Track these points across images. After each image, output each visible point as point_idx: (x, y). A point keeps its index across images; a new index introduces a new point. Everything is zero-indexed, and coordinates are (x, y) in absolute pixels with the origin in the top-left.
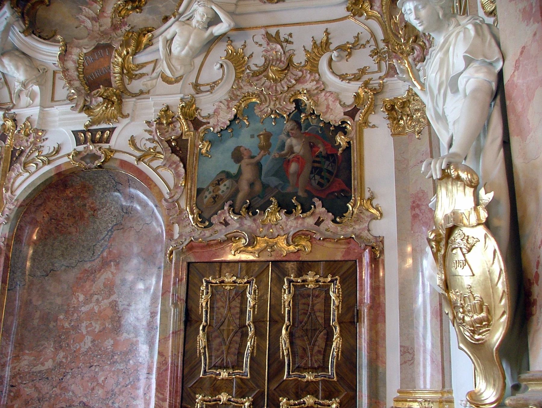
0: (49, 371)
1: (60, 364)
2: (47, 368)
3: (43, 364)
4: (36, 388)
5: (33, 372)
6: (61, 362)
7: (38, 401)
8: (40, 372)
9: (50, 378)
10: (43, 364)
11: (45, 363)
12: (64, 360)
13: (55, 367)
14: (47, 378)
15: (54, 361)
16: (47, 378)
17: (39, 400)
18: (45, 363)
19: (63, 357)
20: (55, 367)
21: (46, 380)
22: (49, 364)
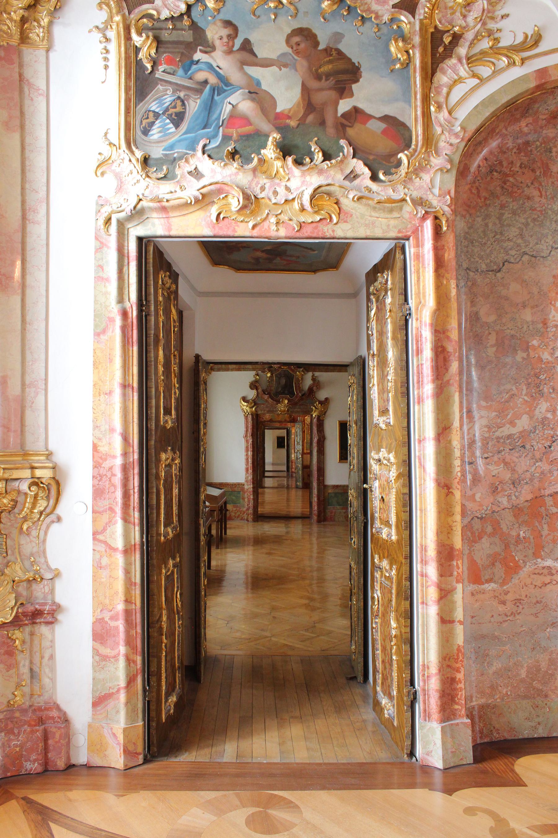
0: (524, 435)
1: (544, 422)
2: (521, 429)
3: (512, 423)
4: (506, 464)
5: (498, 438)
6: (546, 418)
8: (509, 437)
9: (528, 447)
10: (512, 423)
12: (549, 415)
13: (535, 428)
14: (524, 447)
15: (531, 418)
16: (524, 447)
19: (547, 411)
20: (535, 428)
21: (522, 449)
22: (524, 423)
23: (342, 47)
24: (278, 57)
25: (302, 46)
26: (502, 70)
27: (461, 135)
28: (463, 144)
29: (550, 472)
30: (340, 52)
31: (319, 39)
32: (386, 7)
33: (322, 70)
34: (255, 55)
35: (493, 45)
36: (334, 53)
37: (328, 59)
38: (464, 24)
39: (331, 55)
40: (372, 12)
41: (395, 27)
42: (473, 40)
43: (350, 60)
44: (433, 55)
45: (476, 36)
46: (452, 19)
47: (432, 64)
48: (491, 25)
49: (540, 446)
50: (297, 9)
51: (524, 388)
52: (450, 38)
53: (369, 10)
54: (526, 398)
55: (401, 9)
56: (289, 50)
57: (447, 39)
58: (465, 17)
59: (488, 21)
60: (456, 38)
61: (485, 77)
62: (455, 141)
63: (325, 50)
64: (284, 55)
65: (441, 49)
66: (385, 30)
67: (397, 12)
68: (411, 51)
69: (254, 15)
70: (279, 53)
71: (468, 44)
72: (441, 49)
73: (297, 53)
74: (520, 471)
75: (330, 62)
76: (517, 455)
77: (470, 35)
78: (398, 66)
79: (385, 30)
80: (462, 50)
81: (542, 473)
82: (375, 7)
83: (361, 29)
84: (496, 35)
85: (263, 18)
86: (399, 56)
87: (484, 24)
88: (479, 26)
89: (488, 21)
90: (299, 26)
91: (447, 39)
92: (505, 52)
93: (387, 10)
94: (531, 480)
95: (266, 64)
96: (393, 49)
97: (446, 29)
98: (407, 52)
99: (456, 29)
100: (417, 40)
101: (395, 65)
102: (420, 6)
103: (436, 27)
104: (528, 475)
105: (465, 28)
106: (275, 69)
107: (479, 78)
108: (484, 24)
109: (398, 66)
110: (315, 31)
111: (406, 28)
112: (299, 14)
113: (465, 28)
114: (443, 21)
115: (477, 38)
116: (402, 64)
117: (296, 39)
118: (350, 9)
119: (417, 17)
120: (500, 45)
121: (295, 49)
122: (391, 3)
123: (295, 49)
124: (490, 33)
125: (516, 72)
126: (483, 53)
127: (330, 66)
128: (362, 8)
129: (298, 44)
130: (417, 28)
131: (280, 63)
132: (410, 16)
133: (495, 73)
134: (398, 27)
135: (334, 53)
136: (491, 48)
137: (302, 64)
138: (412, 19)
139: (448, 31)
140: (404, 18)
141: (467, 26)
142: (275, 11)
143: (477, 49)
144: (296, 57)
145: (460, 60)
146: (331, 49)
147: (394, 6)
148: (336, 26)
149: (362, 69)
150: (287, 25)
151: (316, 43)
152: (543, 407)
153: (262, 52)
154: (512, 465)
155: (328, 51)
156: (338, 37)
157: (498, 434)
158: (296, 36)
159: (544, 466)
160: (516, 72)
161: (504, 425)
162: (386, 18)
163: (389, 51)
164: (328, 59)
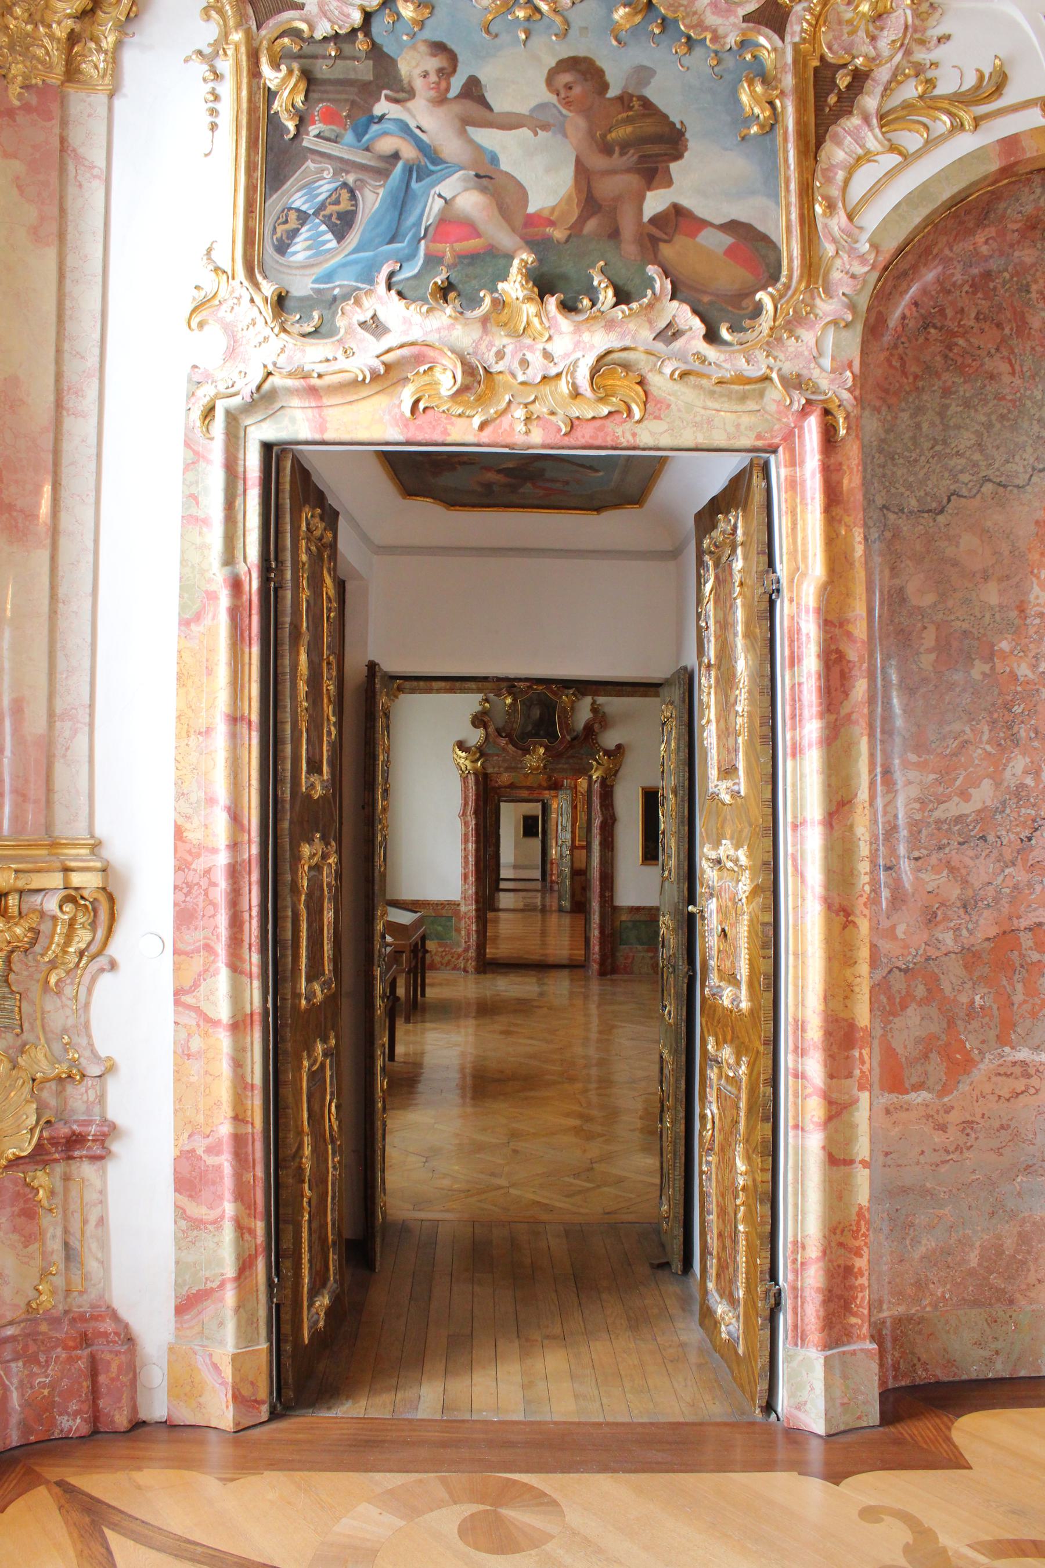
0: (985, 816)
1: (1019, 792)
3: (964, 795)
4: (952, 870)
5: (938, 822)
6: (1022, 786)
7: (961, 911)
8: (959, 819)
9: (991, 838)
10: (964, 795)
11: (971, 791)
12: (1029, 781)
13: (1004, 803)
14: (983, 838)
15: (998, 785)
16: (983, 838)
17: (965, 907)
18: (971, 791)
19: (1026, 772)
20: (1004, 803)
21: (981, 843)
22: (984, 794)
23: (650, 93)
24: (532, 110)
25: (577, 90)
26: (942, 139)
27: (871, 258)
28: (875, 275)
29: (1030, 885)
30: (646, 103)
31: (609, 77)
32: (732, 19)
33: (613, 135)
34: (491, 109)
35: (924, 92)
36: (636, 104)
37: (624, 115)
38: (872, 53)
39: (631, 108)
40: (706, 29)
41: (748, 57)
42: (890, 82)
43: (665, 117)
44: (819, 109)
45: (894, 76)
46: (852, 44)
47: (817, 125)
48: (921, 55)
49: (1012, 837)
50: (567, 22)
51: (986, 729)
52: (848, 79)
53: (700, 25)
54: (988, 748)
55: (759, 23)
56: (553, 98)
57: (843, 81)
58: (873, 39)
60: (860, 78)
61: (911, 151)
62: (860, 269)
63: (620, 99)
64: (542, 107)
65: (832, 99)
66: (730, 62)
67: (751, 30)
68: (778, 103)
69: (488, 32)
70: (533, 103)
71: (879, 89)
72: (832, 99)
73: (568, 103)
74: (977, 885)
75: (629, 121)
76: (971, 853)
77: (883, 74)
78: (754, 129)
79: (730, 62)
80: (870, 102)
81: (1015, 887)
82: (712, 19)
83: (686, 61)
84: (930, 74)
85: (504, 37)
86: (757, 110)
87: (908, 53)
88: (899, 56)
89: (916, 48)
90: (572, 54)
91: (843, 81)
92: (945, 105)
93: (734, 25)
94: (997, 900)
95: (509, 123)
96: (745, 98)
97: (841, 62)
98: (771, 104)
99: (859, 61)
100: (788, 81)
101: (749, 128)
102: (793, 18)
103: (822, 58)
104: (990, 891)
105: (874, 60)
106: (525, 132)
107: (900, 154)
108: (908, 53)
109: (754, 129)
110: (601, 63)
111: (768, 58)
112: (571, 32)
113: (874, 60)
114: (835, 47)
115: (896, 79)
116: (762, 126)
117: (566, 78)
118: (665, 23)
119: (788, 38)
120: (937, 92)
121: (563, 95)
122: (741, 12)
123: (563, 95)
124: (919, 70)
125: (966, 143)
126: (907, 106)
127: (629, 129)
128: (687, 21)
129: (569, 87)
130: (789, 59)
131: (536, 121)
132: (776, 37)
133: (930, 144)
134: (755, 57)
135: (636, 104)
136: (921, 97)
137: (577, 124)
139: (845, 66)
140: (765, 40)
141: (878, 56)
142: (526, 24)
144: (564, 111)
145: (866, 119)
146: (631, 96)
147: (746, 18)
148: (641, 54)
149: (687, 135)
150: (550, 51)
151: (605, 87)
152: (1019, 763)
153: (500, 102)
154: (964, 872)
155: (624, 100)
156: (644, 74)
157: (938, 814)
158: (565, 71)
159: (1018, 874)
160: (966, 143)
161: (949, 798)
162: (732, 40)
163: (738, 101)
164: (624, 115)
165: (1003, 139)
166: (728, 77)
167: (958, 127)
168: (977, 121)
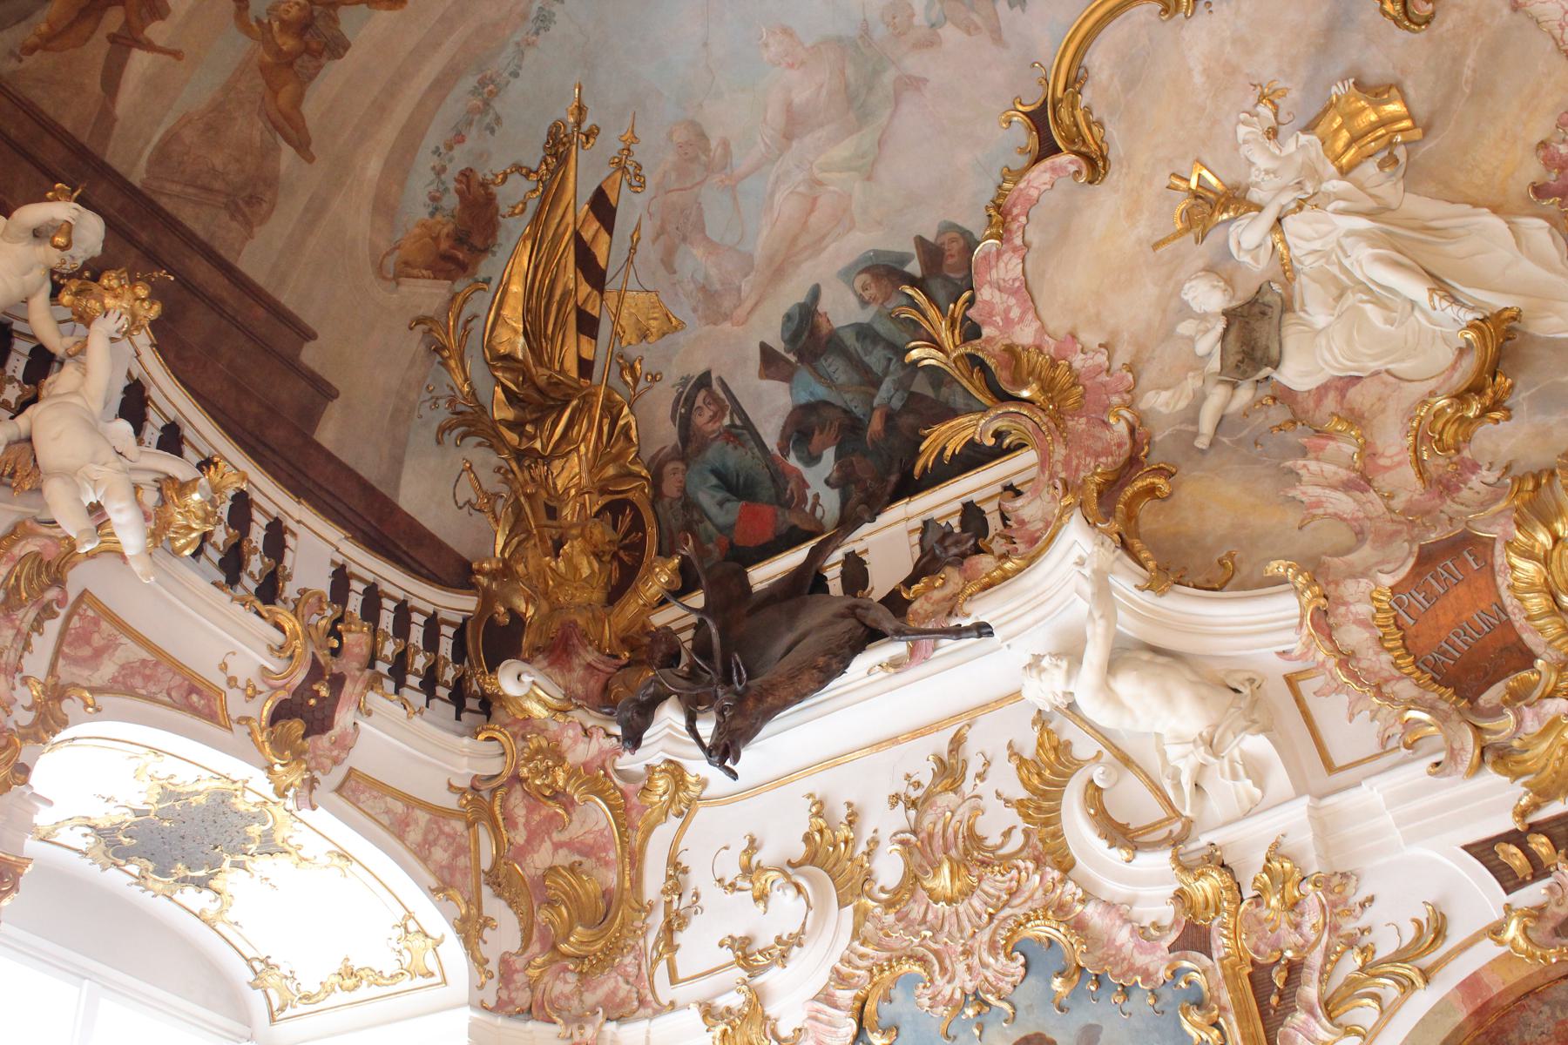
26: (1398, 1005)
32: (1159, 954)
35: (1364, 961)
38: (1301, 941)
40: (1137, 971)
41: (1183, 984)
44: (1264, 1015)
46: (1278, 939)
47: (1266, 1032)
48: (1349, 926)
50: (1013, 1007)
52: (1284, 974)
53: (1133, 969)
55: (1185, 949)
58: (1297, 926)
59: (1341, 921)
60: (1294, 970)
61: (1369, 1026)
65: (1274, 1000)
67: (1179, 958)
68: (1221, 1020)
69: (948, 1037)
71: (1316, 975)
72: (1274, 1000)
77: (1316, 958)
79: (1167, 994)
80: (1311, 991)
82: (1141, 960)
83: (1127, 1007)
85: (963, 1038)
86: (1205, 1036)
87: (1334, 929)
89: (1341, 921)
90: (1022, 1035)
92: (1389, 968)
93: (1162, 958)
96: (1187, 1027)
97: (1272, 960)
98: (1216, 1025)
99: (1289, 954)
100: (1226, 997)
102: (1214, 934)
103: (1253, 962)
105: (1305, 948)
107: (1358, 1034)
108: (1334, 929)
112: (1019, 1013)
113: (1305, 948)
114: (1262, 947)
115: (1331, 959)
118: (1098, 980)
119: (1215, 956)
120: (1378, 957)
122: (1165, 944)
125: (1424, 1000)
126: (1351, 983)
128: (1117, 971)
132: (1204, 957)
133: (1387, 1013)
134: (1189, 983)
136: (1361, 969)
138: (1207, 962)
139: (1277, 963)
140: (1191, 963)
142: (978, 1019)
143: (1338, 980)
145: (1311, 1012)
147: (1171, 949)
160: (1424, 1000)
162: (1163, 974)
165: (1463, 984)
166: (1169, 1010)
167: (1407, 986)
168: (1426, 975)
